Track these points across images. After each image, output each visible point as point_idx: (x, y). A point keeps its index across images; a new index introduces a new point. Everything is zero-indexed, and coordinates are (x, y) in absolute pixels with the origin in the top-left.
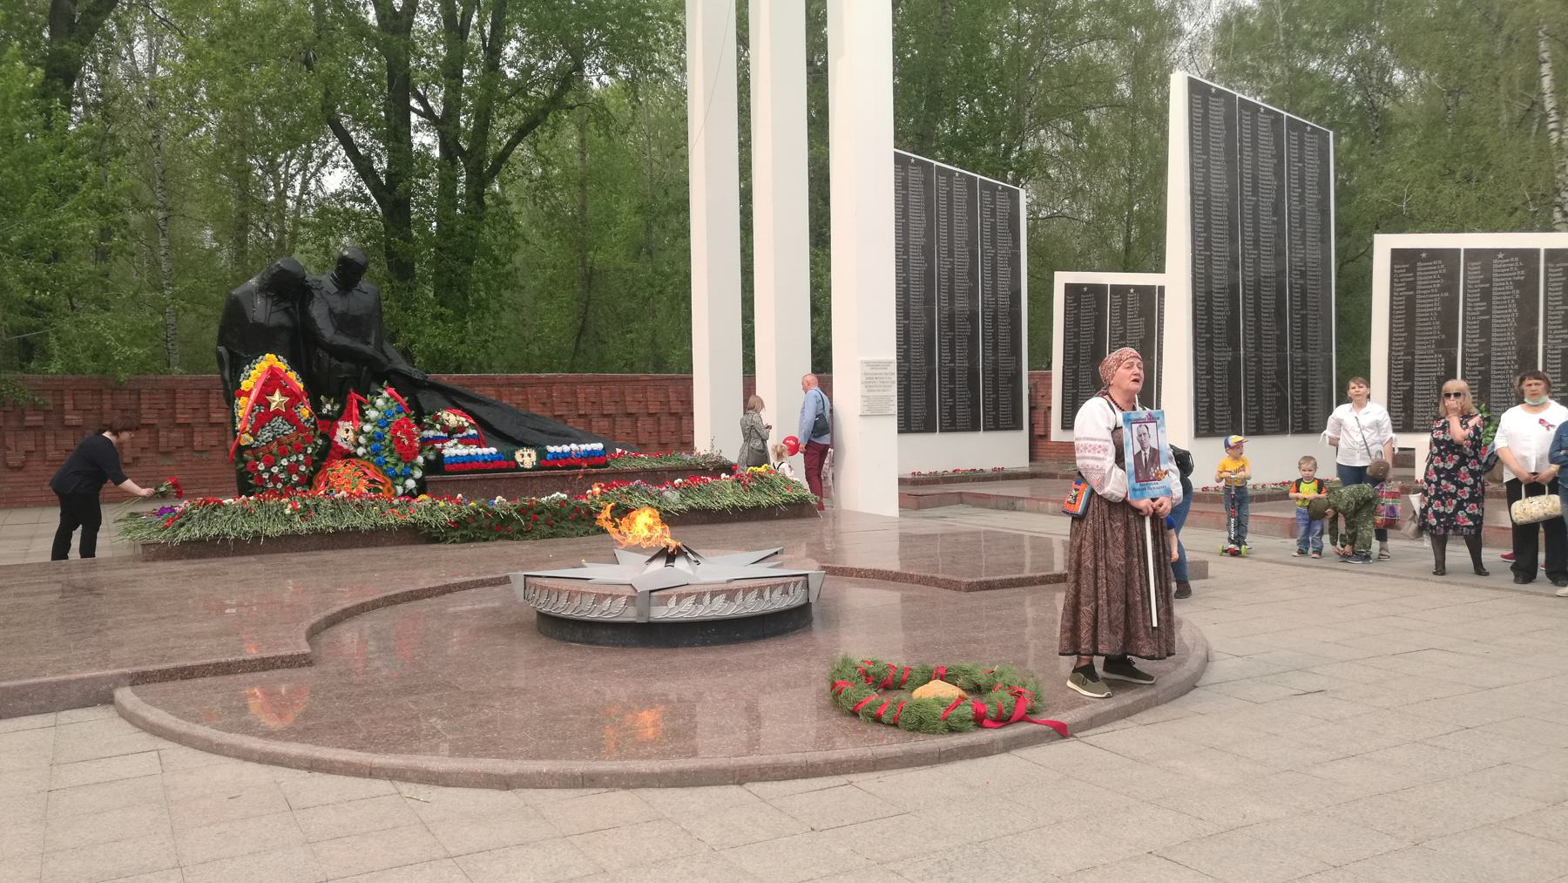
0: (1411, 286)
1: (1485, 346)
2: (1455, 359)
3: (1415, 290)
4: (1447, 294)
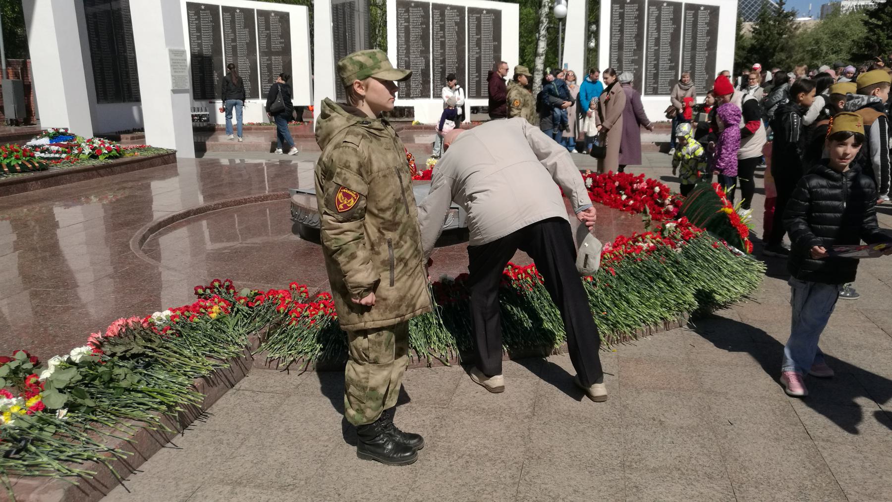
0: (407, 20)
1: (443, 54)
3: (409, 22)
4: (424, 26)
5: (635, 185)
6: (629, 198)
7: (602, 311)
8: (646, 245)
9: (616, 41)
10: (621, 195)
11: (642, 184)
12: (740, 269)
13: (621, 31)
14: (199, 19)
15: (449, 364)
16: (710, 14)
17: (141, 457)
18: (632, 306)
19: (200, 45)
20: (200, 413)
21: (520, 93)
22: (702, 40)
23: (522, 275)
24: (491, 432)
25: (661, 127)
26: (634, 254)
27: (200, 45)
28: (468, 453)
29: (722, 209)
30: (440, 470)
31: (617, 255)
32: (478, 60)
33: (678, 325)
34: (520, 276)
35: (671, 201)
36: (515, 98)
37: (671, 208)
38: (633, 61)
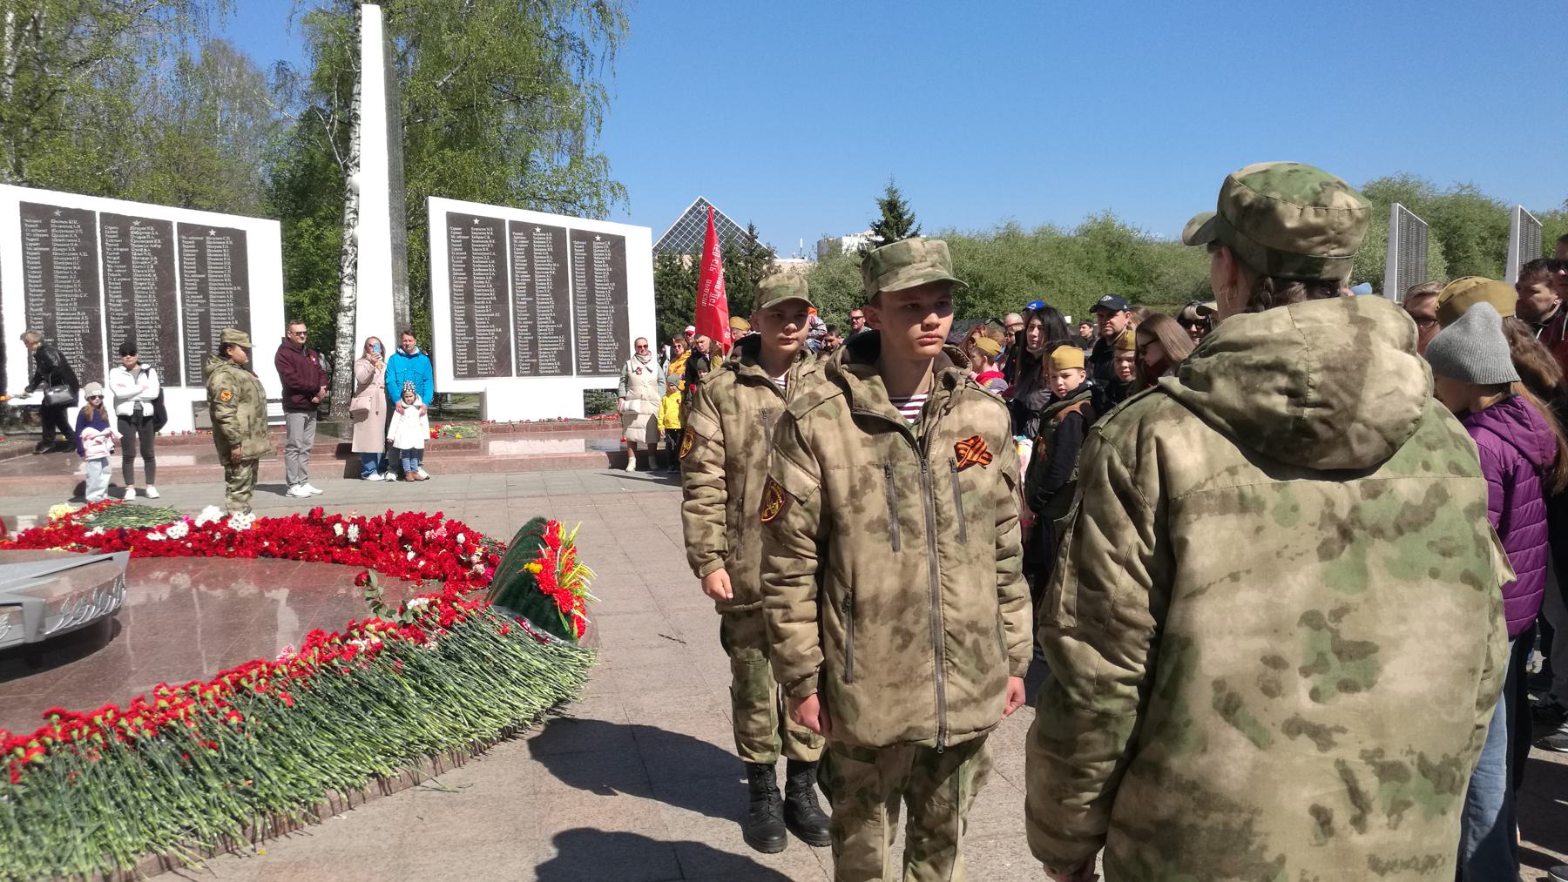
1: (129, 306)
2: (99, 317)
4: (85, 254)
5: (427, 533)
6: (419, 556)
7: (247, 778)
8: (365, 642)
9: (459, 287)
10: (406, 552)
11: (439, 530)
12: (542, 667)
13: (468, 270)
16: (611, 247)
18: (313, 760)
21: (233, 378)
22: (603, 288)
23: (80, 730)
25: (547, 429)
26: (335, 662)
29: (526, 566)
31: (302, 668)
32: (204, 319)
33: (411, 783)
34: (75, 733)
35: (482, 558)
36: (222, 386)
37: (481, 568)
38: (492, 321)
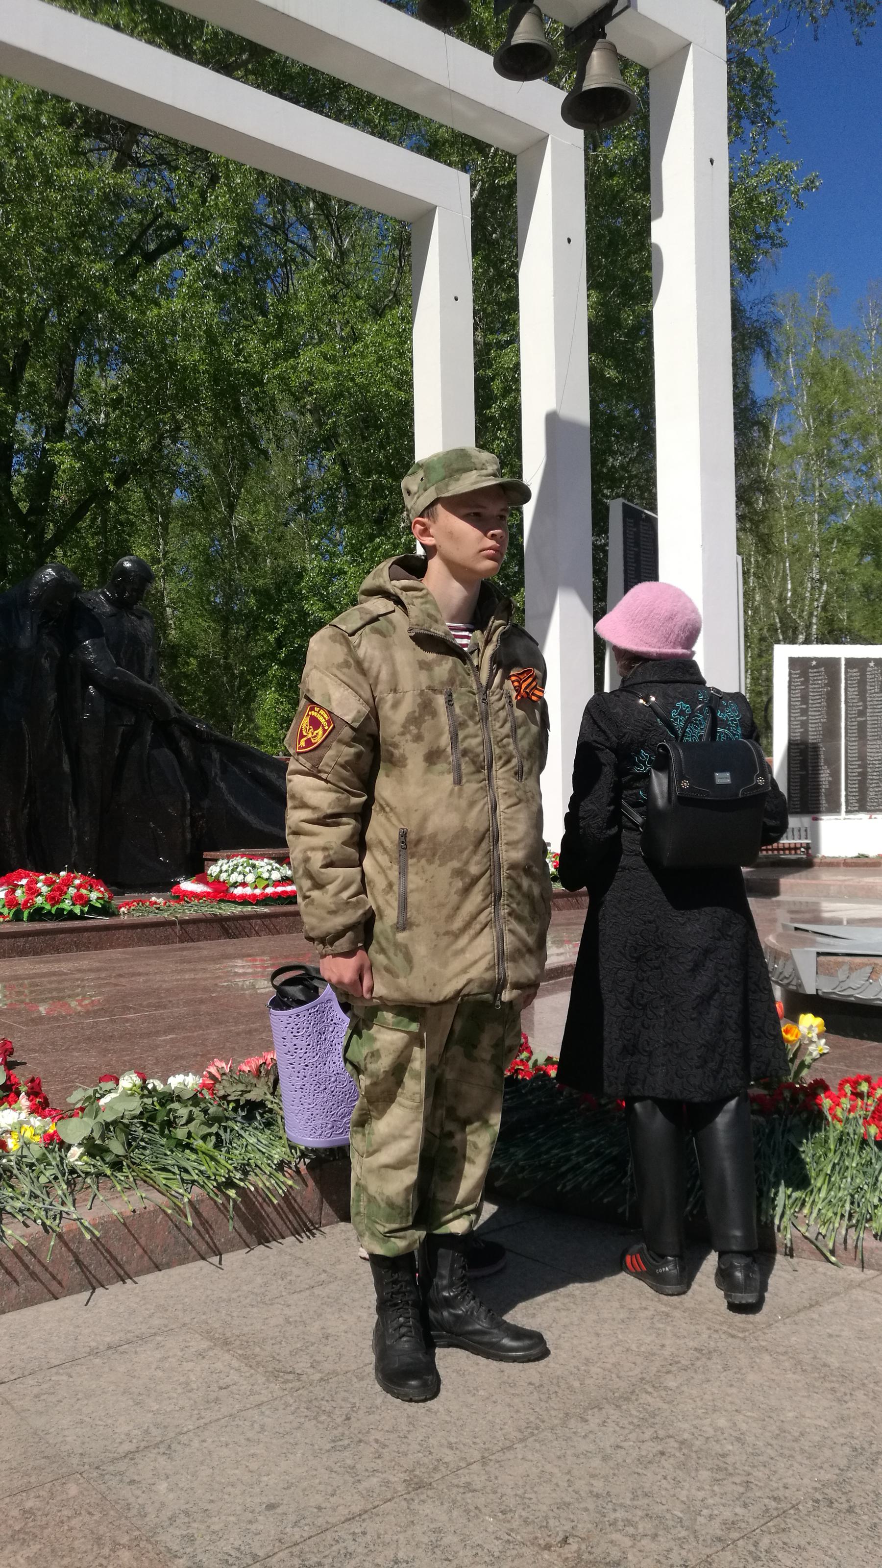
14: (806, 682)
15: (833, 1259)
17: (146, 1258)
19: (804, 724)
20: (305, 1224)
24: (791, 1414)
27: (804, 724)
28: (686, 1436)
30: (584, 1446)
